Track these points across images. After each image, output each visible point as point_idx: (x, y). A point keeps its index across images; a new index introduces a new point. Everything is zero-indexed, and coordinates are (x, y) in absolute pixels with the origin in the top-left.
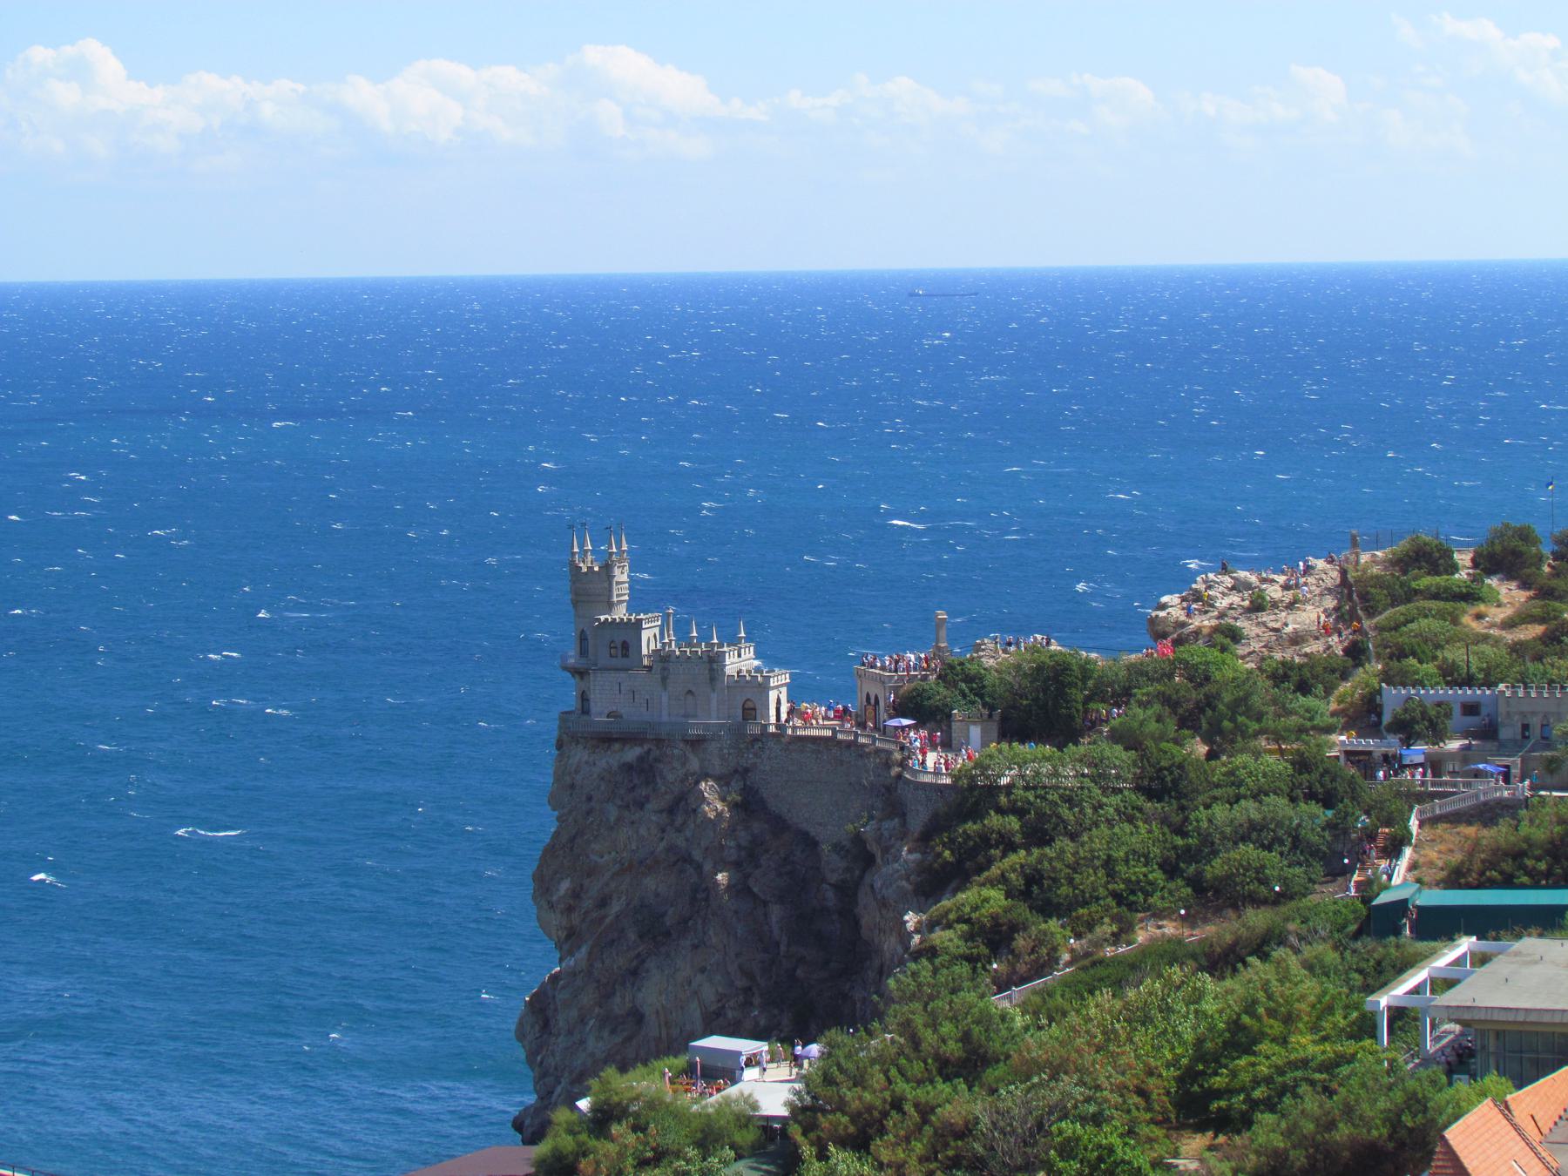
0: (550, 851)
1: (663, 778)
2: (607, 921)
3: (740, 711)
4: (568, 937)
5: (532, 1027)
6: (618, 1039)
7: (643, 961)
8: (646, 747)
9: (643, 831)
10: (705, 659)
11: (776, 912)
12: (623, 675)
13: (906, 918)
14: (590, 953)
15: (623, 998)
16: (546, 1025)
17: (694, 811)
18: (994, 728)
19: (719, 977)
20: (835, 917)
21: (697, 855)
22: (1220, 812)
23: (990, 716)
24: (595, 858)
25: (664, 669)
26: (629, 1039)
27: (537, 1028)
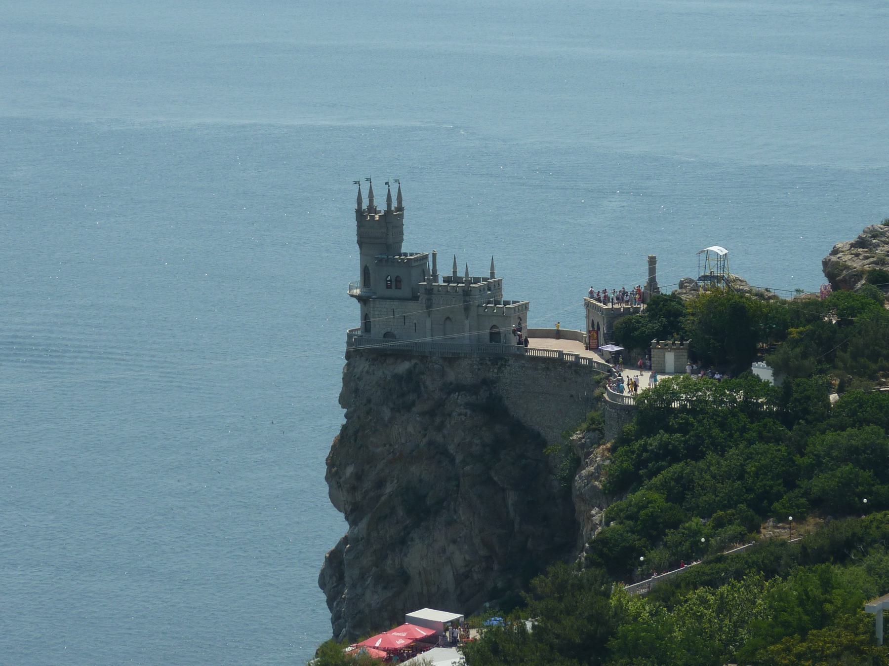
2: (383, 499)
4: (353, 511)
5: (331, 578)
7: (409, 533)
8: (413, 362)
9: (410, 429)
11: (512, 497)
12: (396, 303)
13: (593, 512)
16: (341, 578)
17: (450, 415)
18: (685, 353)
19: (466, 547)
21: (451, 449)
22: (830, 437)
25: (429, 300)
27: (334, 578)
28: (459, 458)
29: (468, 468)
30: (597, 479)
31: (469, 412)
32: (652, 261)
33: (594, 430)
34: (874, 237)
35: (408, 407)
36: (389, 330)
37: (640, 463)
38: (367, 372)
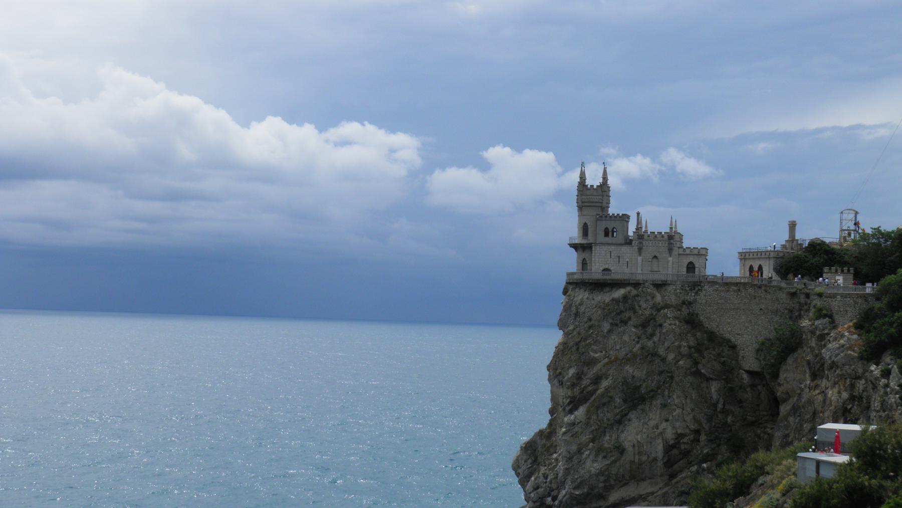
1: (640, 306)
2: (599, 392)
3: (685, 269)
6: (608, 462)
7: (627, 414)
9: (626, 338)
10: (666, 237)
11: (714, 387)
14: (588, 411)
15: (611, 436)
17: (661, 325)
20: (748, 390)
21: (661, 351)
23: (849, 270)
24: (592, 354)
26: (614, 462)
27: (530, 461)
28: (671, 357)
29: (681, 363)
31: (678, 323)
32: (793, 226)
35: (625, 322)
36: (607, 267)
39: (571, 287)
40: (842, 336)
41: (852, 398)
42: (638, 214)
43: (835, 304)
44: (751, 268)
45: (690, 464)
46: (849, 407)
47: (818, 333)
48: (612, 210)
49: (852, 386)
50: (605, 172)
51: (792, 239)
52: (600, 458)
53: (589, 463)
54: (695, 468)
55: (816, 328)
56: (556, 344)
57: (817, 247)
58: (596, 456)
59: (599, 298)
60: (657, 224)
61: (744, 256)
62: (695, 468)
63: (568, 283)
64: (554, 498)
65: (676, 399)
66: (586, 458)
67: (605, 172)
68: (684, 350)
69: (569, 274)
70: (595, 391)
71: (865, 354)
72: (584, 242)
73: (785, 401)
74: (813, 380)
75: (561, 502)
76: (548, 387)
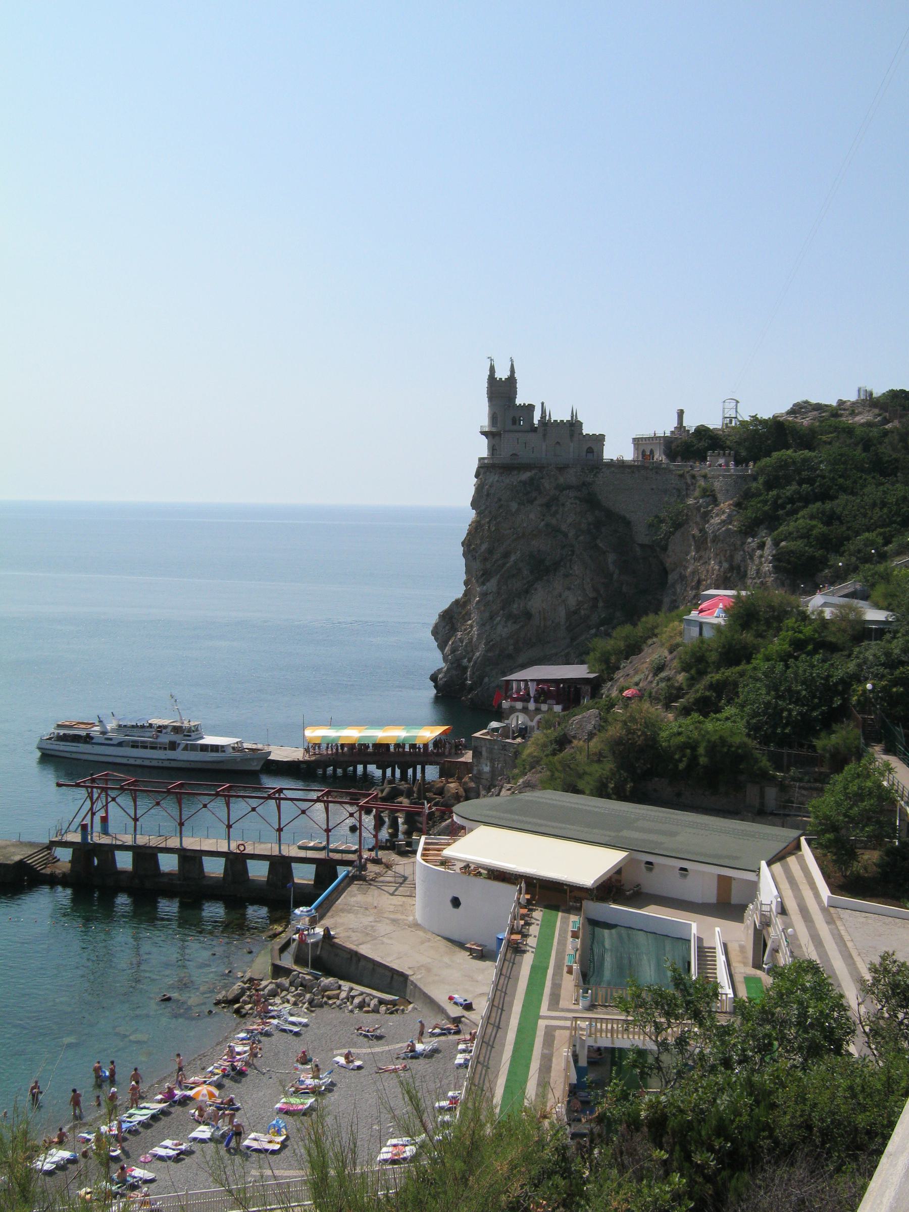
0: (475, 530)
4: (483, 575)
6: (517, 627)
8: (533, 472)
9: (532, 516)
11: (611, 558)
12: (520, 434)
14: (499, 582)
15: (519, 604)
17: (563, 505)
21: (564, 527)
25: (545, 430)
27: (447, 628)
29: (581, 538)
30: (730, 523)
31: (578, 502)
32: (681, 414)
33: (708, 496)
34: (801, 408)
37: (776, 506)
38: (498, 481)
39: (482, 471)
40: (724, 512)
41: (732, 568)
42: (543, 404)
43: (717, 485)
44: (644, 451)
45: (589, 628)
46: (729, 575)
47: (702, 510)
48: (519, 401)
49: (732, 557)
50: (512, 366)
51: (680, 426)
52: (509, 624)
53: (499, 629)
54: (593, 631)
55: (701, 506)
56: (470, 523)
57: (702, 431)
58: (506, 622)
59: (508, 481)
60: (560, 414)
61: (637, 442)
62: (593, 631)
63: (479, 468)
64: (469, 661)
65: (577, 569)
66: (497, 624)
67: (512, 366)
68: (584, 526)
69: (481, 459)
70: (504, 564)
71: (743, 528)
72: (494, 430)
73: (673, 570)
74: (697, 552)
75: (475, 663)
76: (463, 561)
